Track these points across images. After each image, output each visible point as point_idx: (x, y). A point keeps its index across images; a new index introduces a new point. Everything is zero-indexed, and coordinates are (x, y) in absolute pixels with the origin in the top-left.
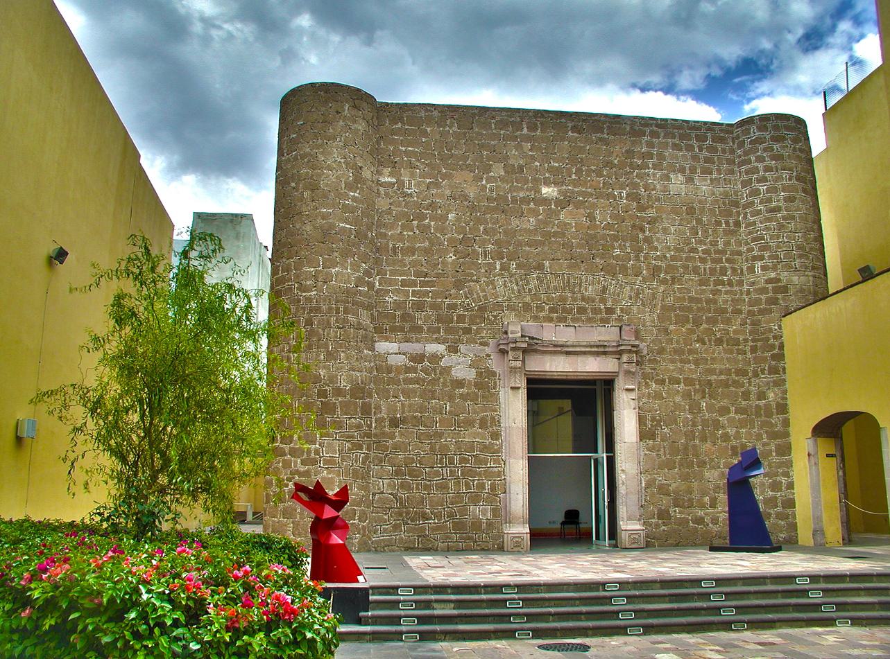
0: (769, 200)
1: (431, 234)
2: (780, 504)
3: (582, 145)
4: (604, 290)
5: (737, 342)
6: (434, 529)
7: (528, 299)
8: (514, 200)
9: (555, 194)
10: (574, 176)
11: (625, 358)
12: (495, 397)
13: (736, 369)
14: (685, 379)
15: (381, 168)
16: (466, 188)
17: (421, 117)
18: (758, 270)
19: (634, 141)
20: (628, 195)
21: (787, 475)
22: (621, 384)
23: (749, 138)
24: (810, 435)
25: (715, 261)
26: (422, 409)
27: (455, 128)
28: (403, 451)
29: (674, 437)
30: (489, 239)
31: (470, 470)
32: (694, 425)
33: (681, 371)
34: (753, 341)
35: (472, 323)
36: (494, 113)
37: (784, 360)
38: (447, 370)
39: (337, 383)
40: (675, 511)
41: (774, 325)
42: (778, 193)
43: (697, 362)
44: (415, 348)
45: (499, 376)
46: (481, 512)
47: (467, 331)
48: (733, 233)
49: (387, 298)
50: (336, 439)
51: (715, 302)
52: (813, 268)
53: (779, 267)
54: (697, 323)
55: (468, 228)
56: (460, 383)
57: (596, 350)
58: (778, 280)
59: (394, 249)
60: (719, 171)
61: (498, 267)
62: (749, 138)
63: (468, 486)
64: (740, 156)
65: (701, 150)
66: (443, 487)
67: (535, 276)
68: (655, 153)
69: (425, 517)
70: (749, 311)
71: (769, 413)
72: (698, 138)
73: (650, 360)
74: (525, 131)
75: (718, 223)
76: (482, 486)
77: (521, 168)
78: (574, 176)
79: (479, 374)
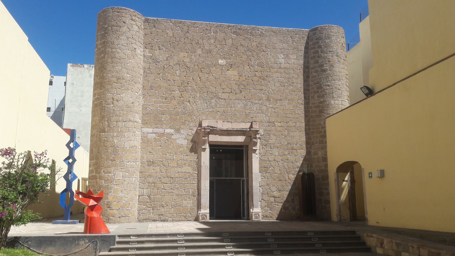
1: (168, 80)
9: (225, 63)
18: (316, 97)
23: (315, 37)
44: (161, 130)
45: (198, 143)
49: (147, 109)
50: (121, 171)
56: (180, 146)
62: (315, 37)
74: (212, 33)
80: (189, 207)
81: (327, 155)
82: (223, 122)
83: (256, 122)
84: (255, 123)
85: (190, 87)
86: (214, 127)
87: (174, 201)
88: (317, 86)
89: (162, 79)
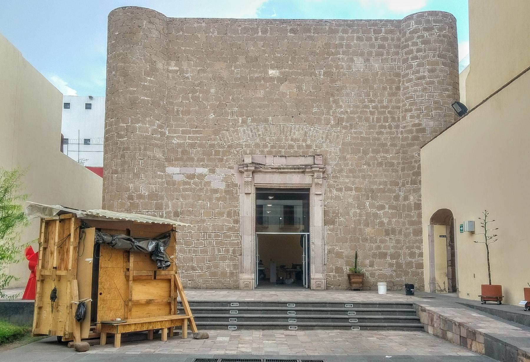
0: (418, 72)
1: (200, 101)
2: (414, 266)
3: (297, 41)
5: (392, 165)
7: (258, 140)
8: (252, 79)
9: (277, 74)
10: (290, 63)
11: (316, 175)
12: (237, 199)
13: (390, 181)
14: (356, 188)
15: (170, 61)
16: (222, 72)
17: (195, 27)
18: (408, 118)
20: (325, 73)
21: (419, 248)
22: (314, 191)
23: (409, 30)
24: (429, 224)
25: (380, 113)
26: (193, 206)
27: (216, 34)
28: (181, 230)
29: (347, 223)
30: (235, 104)
31: (221, 242)
33: (353, 183)
34: (403, 163)
35: (224, 155)
36: (240, 23)
37: (420, 176)
38: (208, 183)
39: (140, 191)
40: (346, 268)
41: (416, 154)
42: (425, 67)
43: (364, 177)
44: (190, 170)
45: (239, 187)
46: (226, 266)
47: (221, 160)
51: (379, 139)
52: (445, 116)
53: (421, 116)
54: (365, 153)
55: (222, 98)
56: (216, 191)
58: (419, 125)
59: (178, 111)
61: (240, 121)
63: (219, 251)
64: (403, 43)
65: (376, 39)
66: (204, 252)
67: (263, 126)
68: (345, 44)
69: (193, 269)
70: (402, 144)
71: (410, 210)
72: (375, 32)
73: (333, 176)
74: (260, 34)
75: (384, 89)
76: (227, 251)
77: (256, 59)
78: (290, 63)
79: (228, 186)
81: (421, 200)
83: (320, 156)
85: (229, 109)
86: (262, 165)
87: (209, 263)
88: (410, 101)
89: (192, 101)
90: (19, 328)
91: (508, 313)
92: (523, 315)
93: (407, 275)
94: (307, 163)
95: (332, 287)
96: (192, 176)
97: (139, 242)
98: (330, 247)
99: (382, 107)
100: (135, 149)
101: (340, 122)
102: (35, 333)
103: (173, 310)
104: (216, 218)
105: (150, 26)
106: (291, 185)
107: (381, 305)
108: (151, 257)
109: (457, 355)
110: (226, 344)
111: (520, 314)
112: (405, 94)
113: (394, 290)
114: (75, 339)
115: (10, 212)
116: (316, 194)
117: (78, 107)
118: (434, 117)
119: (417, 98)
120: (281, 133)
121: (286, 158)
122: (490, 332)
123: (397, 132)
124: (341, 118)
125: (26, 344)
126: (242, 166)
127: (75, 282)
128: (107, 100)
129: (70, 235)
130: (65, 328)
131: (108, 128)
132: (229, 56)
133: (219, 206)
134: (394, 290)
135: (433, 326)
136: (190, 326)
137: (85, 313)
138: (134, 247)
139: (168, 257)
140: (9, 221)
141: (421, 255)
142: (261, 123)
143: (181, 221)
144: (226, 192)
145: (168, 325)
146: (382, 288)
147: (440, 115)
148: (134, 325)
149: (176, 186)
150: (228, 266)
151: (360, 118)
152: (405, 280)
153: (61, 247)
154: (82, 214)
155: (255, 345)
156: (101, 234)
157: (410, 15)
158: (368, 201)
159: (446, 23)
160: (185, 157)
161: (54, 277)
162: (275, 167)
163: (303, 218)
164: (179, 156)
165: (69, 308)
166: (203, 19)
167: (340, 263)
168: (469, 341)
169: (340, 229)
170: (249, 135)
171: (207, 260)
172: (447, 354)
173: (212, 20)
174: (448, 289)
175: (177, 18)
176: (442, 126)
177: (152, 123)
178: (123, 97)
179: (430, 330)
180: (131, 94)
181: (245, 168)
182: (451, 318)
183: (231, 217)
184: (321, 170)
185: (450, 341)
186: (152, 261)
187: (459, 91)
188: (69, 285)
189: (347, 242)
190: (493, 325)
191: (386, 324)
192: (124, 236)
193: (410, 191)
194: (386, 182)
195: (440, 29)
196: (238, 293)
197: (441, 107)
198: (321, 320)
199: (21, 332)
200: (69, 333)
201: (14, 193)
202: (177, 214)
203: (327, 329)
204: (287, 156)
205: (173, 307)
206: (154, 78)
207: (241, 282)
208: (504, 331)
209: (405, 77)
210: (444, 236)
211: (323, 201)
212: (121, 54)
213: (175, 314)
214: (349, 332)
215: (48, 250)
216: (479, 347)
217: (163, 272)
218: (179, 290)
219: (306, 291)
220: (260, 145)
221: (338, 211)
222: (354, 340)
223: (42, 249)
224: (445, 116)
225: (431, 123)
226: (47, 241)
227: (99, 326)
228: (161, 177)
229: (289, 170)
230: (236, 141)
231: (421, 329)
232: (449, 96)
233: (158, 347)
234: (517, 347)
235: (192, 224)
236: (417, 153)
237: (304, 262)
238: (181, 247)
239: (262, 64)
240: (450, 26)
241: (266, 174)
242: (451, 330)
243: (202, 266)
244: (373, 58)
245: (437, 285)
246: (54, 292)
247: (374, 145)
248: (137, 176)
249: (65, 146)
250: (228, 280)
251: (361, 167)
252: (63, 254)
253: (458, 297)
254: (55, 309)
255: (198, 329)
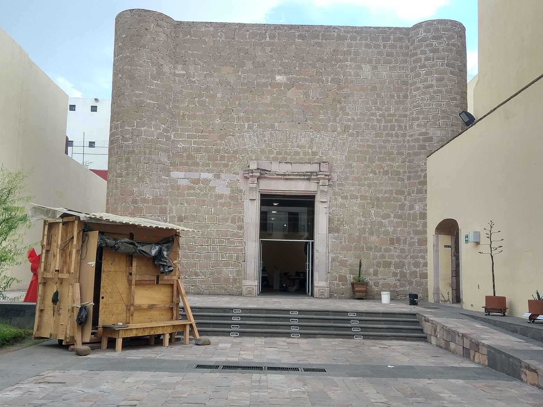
1: (206, 106)
2: (418, 276)
3: (304, 47)
4: (312, 141)
5: (398, 173)
6: (201, 282)
8: (259, 85)
9: (285, 80)
10: (297, 69)
11: (321, 182)
12: (241, 205)
14: (361, 196)
15: (176, 65)
16: (229, 77)
17: (202, 31)
19: (340, 43)
21: (424, 258)
22: (318, 199)
23: (418, 38)
25: (387, 121)
27: (223, 38)
28: (185, 235)
30: (242, 110)
31: (225, 247)
32: (365, 224)
33: (359, 191)
34: (409, 172)
36: (248, 28)
38: (213, 188)
40: (350, 277)
41: (422, 163)
42: (433, 76)
43: (369, 186)
44: (194, 175)
45: (244, 193)
46: (228, 272)
47: (226, 165)
48: (402, 103)
51: (385, 148)
52: (452, 125)
54: (372, 161)
55: (229, 102)
56: (220, 196)
57: (303, 177)
58: (427, 133)
59: (184, 115)
60: (396, 61)
61: (246, 127)
62: (418, 38)
64: (411, 51)
65: (385, 47)
67: (269, 132)
68: (353, 51)
69: (196, 274)
70: (408, 153)
71: (415, 219)
72: (384, 39)
73: (338, 184)
74: (268, 39)
75: (392, 96)
76: (231, 257)
77: (264, 64)
78: (297, 69)
79: (232, 191)
80: (232, 278)
82: (280, 163)
83: (326, 163)
84: (324, 164)
86: (267, 171)
87: (212, 268)
88: (417, 109)
89: (198, 105)
90: (19, 330)
91: (512, 325)
92: (527, 327)
93: (411, 284)
94: (312, 170)
95: (335, 295)
96: (197, 181)
97: (143, 246)
98: (334, 255)
99: (388, 115)
100: (140, 152)
101: (346, 130)
102: (36, 336)
103: (175, 315)
104: (220, 224)
105: (158, 29)
106: (296, 192)
107: (384, 314)
108: (154, 262)
109: (460, 366)
110: (228, 351)
111: (524, 326)
112: (412, 102)
113: (397, 300)
114: (76, 342)
115: (13, 214)
116: (321, 202)
117: (83, 109)
118: (441, 126)
119: (424, 106)
120: (287, 140)
121: (292, 165)
122: (493, 344)
123: (404, 140)
124: (348, 125)
125: (27, 347)
126: (247, 172)
127: (77, 285)
128: (113, 103)
129: (73, 238)
130: (66, 332)
131: (113, 131)
132: (236, 61)
133: (223, 212)
134: (397, 300)
135: (436, 336)
136: (192, 332)
137: (87, 316)
138: (137, 251)
139: (171, 262)
140: (12, 223)
141: (425, 265)
142: (268, 129)
143: (185, 226)
144: (230, 197)
145: (170, 331)
146: (385, 297)
147: (447, 125)
148: (135, 330)
149: (180, 191)
150: (232, 272)
151: (367, 126)
152: (409, 289)
153: (64, 250)
154: (85, 216)
155: (256, 352)
156: (104, 237)
157: (419, 23)
158: (373, 209)
159: (455, 32)
160: (190, 162)
161: (56, 279)
162: (280, 173)
163: (308, 225)
164: (184, 161)
165: (70, 311)
166: (211, 23)
167: (344, 271)
168: (472, 353)
169: (345, 237)
170: (255, 140)
171: (210, 266)
172: (450, 365)
173: (219, 25)
174: (452, 300)
175: (184, 22)
176: (449, 135)
177: (157, 127)
178: (129, 100)
179: (433, 340)
180: (137, 98)
181: (251, 174)
182: (454, 329)
183: (235, 223)
184: (327, 177)
185: (453, 352)
186: (155, 265)
187: (467, 100)
188: (71, 288)
189: (351, 250)
190: (495, 337)
191: (389, 334)
192: (127, 240)
193: (416, 200)
194: (392, 191)
195: (449, 38)
196: (240, 299)
197: (448, 117)
198: (323, 328)
199: (22, 334)
200: (70, 337)
201: (17, 195)
202: (181, 219)
203: (330, 338)
204: (292, 162)
205: (175, 312)
206: (160, 82)
207: (244, 288)
208: (508, 343)
209: (412, 85)
210: (449, 247)
211: (328, 209)
212: (128, 57)
213: (177, 319)
214: (352, 340)
215: (51, 252)
216: (482, 358)
217: (166, 277)
218: (182, 295)
219: (309, 299)
220: (265, 151)
221: (343, 219)
222: (358, 350)
223: (44, 251)
224: (452, 125)
225: (438, 133)
226: (50, 244)
227: (100, 330)
228: (165, 181)
229: (295, 177)
230: (241, 147)
231: (424, 339)
232: (456, 106)
233: (160, 352)
234: (520, 359)
235: (195, 229)
236: (423, 162)
237: (308, 270)
238: (184, 252)
239: (269, 70)
240: (459, 35)
241: (272, 180)
242: (454, 341)
243: (205, 272)
244: (381, 65)
245: (441, 295)
246: (56, 294)
247: (381, 153)
248: (141, 179)
249: (70, 148)
250: (231, 286)
251: (367, 175)
252: (66, 257)
253: (462, 308)
254: (56, 312)
255: (200, 335)
